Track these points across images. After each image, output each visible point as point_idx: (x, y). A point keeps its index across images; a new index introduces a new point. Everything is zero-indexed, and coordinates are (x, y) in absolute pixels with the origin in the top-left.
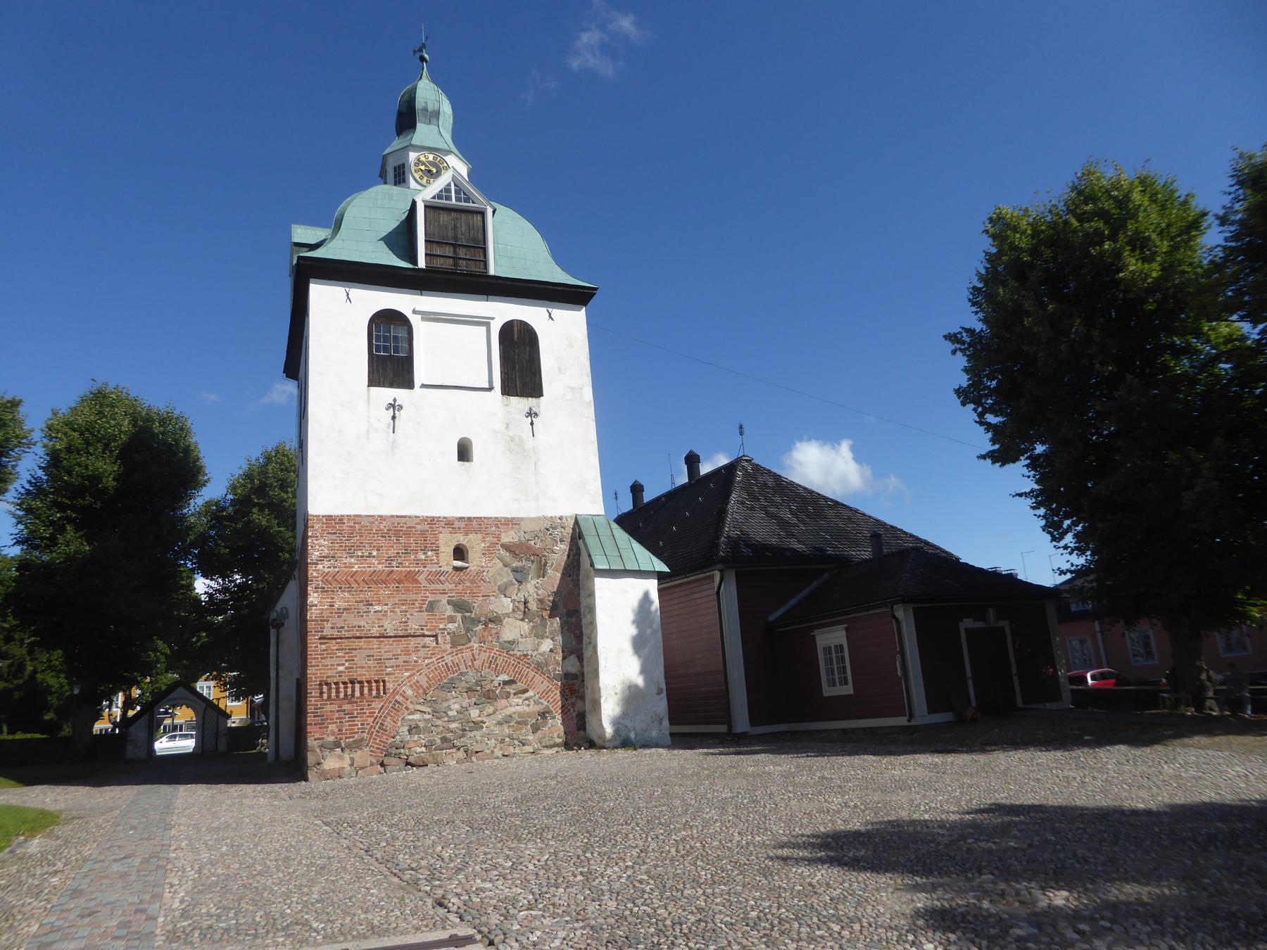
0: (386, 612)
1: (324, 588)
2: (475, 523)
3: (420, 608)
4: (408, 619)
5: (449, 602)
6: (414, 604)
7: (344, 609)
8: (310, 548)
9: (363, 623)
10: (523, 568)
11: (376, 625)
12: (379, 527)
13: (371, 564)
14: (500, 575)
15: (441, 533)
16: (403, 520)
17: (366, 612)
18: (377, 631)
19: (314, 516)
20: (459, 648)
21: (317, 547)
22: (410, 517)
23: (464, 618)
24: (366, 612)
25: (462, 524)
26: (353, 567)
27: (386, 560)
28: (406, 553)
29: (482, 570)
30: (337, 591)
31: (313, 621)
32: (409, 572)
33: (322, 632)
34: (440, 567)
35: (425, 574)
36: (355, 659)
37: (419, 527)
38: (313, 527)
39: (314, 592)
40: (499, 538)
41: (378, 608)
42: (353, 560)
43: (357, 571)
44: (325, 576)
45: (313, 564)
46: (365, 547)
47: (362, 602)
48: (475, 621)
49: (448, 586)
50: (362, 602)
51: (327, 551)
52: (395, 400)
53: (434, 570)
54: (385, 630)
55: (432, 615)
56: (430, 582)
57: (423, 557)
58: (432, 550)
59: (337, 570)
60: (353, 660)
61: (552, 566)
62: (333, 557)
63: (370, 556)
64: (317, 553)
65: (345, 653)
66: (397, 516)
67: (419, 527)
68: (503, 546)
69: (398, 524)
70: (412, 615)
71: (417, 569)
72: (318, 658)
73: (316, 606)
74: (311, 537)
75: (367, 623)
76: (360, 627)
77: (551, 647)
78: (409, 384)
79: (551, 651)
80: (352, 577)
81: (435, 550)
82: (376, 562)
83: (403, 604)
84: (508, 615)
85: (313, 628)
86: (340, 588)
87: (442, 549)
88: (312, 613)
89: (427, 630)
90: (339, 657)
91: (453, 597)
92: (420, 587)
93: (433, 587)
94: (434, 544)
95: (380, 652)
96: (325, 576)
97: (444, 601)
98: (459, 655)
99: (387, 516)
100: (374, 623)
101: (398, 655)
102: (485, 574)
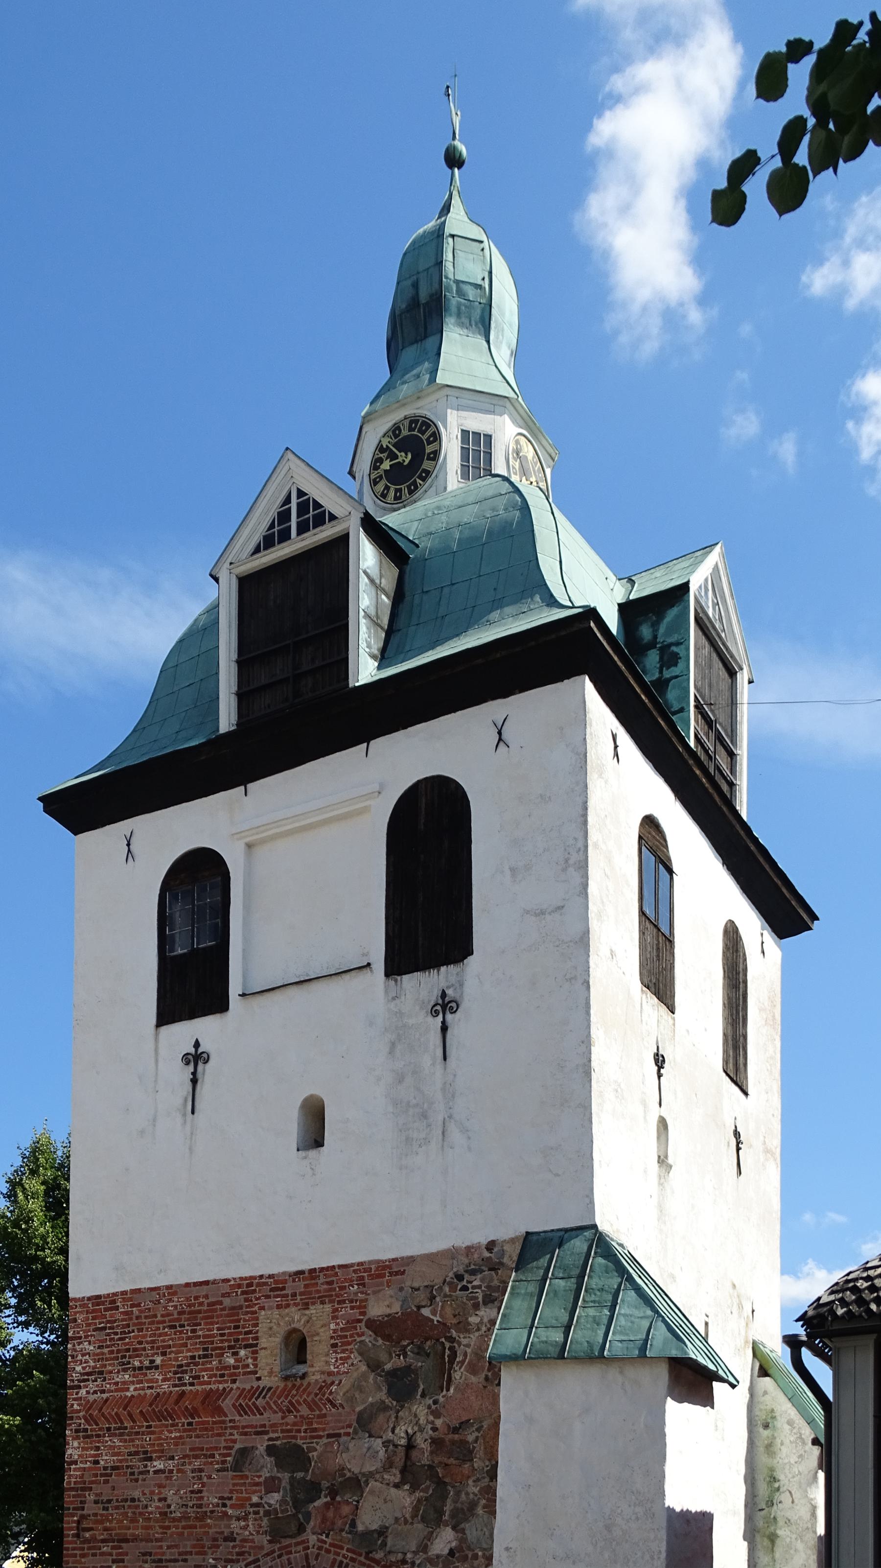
0: (171, 1471)
1: (86, 1430)
2: (322, 1280)
3: (224, 1462)
4: (203, 1485)
5: (271, 1450)
6: (213, 1456)
7: (114, 1468)
8: (70, 1359)
9: (137, 1494)
10: (408, 1370)
11: (156, 1498)
12: (166, 1307)
13: (151, 1381)
14: (361, 1390)
15: (262, 1308)
16: (204, 1290)
17: (141, 1473)
18: (157, 1507)
19: (75, 1300)
20: (286, 1542)
21: (80, 1357)
22: (214, 1282)
23: (292, 1479)
24: (141, 1473)
25: (300, 1286)
26: (128, 1390)
27: (175, 1373)
28: (205, 1356)
29: (329, 1380)
30: (104, 1436)
31: (72, 1489)
32: (209, 1394)
33: (83, 1508)
34: (259, 1379)
35: (235, 1394)
36: (126, 1558)
37: (227, 1302)
38: (75, 1320)
39: (74, 1439)
40: (362, 1308)
41: (159, 1465)
42: (127, 1377)
43: (132, 1396)
44: (89, 1409)
45: (73, 1388)
46: (144, 1349)
47: (136, 1453)
48: (313, 1490)
49: (270, 1417)
50: (136, 1453)
51: (92, 1364)
52: (197, 1045)
53: (248, 1387)
54: (169, 1506)
55: (242, 1477)
56: (242, 1410)
57: (232, 1361)
58: (246, 1347)
59: (105, 1396)
60: (123, 1561)
61: (463, 1362)
62: (101, 1373)
63: (153, 1366)
64: (79, 1368)
65: (113, 1548)
66: (196, 1284)
67: (227, 1302)
68: (371, 1324)
69: (196, 1298)
70: (209, 1477)
71: (221, 1387)
72: (75, 1556)
73: (76, 1463)
74: (73, 1338)
75: (144, 1494)
76: (133, 1500)
77: (454, 1544)
78: (220, 1005)
79: (452, 1553)
80: (125, 1409)
81: (251, 1346)
82: (160, 1378)
83: (196, 1457)
84: (371, 1475)
85: (72, 1502)
86: (109, 1429)
87: (263, 1342)
88: (70, 1476)
89: (232, 1507)
90: (102, 1554)
91: (277, 1439)
92: (224, 1422)
93: (245, 1420)
94: (250, 1332)
95: (161, 1547)
96: (89, 1409)
97: (262, 1449)
98: (285, 1557)
99: (179, 1286)
100: (152, 1493)
101: (186, 1553)
102: (334, 1388)
